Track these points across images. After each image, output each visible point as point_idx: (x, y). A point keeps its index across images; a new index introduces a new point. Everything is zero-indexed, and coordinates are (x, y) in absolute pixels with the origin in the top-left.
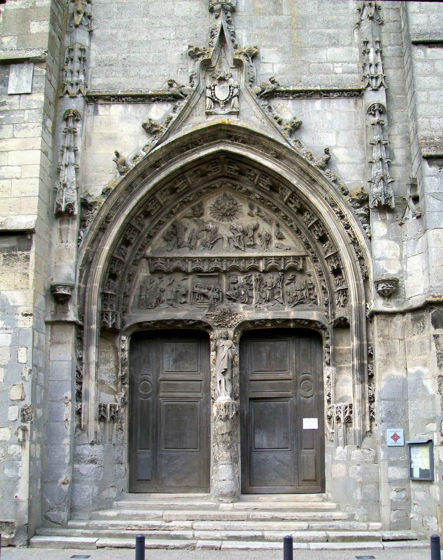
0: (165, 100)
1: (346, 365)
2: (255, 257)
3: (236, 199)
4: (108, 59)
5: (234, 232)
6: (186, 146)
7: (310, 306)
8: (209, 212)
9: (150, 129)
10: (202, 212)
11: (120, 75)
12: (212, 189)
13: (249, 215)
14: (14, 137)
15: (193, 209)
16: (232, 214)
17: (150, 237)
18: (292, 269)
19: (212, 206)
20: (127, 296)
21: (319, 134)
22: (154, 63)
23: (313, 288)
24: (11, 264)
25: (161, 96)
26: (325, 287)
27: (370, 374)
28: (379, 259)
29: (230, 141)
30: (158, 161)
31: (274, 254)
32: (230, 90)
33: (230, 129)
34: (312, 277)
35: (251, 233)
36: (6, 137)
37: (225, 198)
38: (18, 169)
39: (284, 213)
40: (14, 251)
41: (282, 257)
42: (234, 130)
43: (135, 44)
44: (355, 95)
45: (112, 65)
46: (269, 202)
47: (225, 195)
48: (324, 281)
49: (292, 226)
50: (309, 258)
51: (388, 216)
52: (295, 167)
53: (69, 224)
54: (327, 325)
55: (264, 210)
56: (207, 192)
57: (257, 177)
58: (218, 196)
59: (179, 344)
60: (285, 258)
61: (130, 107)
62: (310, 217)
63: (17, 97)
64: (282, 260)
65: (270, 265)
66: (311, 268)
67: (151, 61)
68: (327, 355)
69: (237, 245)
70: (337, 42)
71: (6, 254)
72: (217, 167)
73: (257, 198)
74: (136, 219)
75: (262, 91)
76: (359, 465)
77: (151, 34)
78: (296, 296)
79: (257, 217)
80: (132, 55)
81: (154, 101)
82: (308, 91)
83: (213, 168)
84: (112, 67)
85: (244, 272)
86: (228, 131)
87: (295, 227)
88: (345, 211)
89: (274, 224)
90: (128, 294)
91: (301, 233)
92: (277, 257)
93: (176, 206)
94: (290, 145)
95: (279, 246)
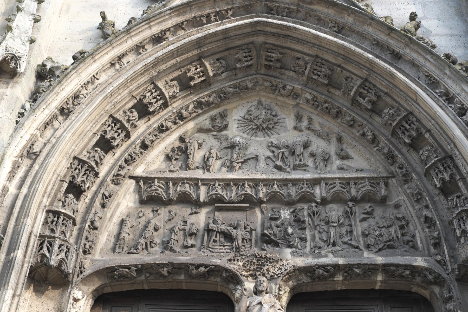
3: (277, 108)
7: (406, 251)
8: (236, 126)
10: (225, 123)
12: (241, 91)
13: (295, 128)
15: (213, 119)
16: (270, 126)
17: (144, 146)
20: (96, 228)
21: (397, 6)
23: (407, 224)
26: (429, 215)
30: (165, 31)
31: (337, 175)
34: (403, 208)
35: (299, 150)
37: (260, 107)
39: (350, 116)
41: (350, 179)
46: (325, 102)
47: (260, 103)
48: (427, 207)
49: (364, 135)
50: (394, 180)
52: (367, 43)
54: (444, 275)
55: (319, 121)
56: (234, 94)
57: (309, 66)
62: (395, 112)
64: (352, 184)
65: (332, 191)
66: (399, 195)
69: (279, 163)
73: (307, 101)
74: (125, 112)
78: (381, 235)
79: (308, 132)
85: (289, 204)
87: (369, 133)
89: (334, 139)
90: (97, 224)
91: (379, 143)
92: (344, 179)
93: (188, 106)
95: (345, 167)
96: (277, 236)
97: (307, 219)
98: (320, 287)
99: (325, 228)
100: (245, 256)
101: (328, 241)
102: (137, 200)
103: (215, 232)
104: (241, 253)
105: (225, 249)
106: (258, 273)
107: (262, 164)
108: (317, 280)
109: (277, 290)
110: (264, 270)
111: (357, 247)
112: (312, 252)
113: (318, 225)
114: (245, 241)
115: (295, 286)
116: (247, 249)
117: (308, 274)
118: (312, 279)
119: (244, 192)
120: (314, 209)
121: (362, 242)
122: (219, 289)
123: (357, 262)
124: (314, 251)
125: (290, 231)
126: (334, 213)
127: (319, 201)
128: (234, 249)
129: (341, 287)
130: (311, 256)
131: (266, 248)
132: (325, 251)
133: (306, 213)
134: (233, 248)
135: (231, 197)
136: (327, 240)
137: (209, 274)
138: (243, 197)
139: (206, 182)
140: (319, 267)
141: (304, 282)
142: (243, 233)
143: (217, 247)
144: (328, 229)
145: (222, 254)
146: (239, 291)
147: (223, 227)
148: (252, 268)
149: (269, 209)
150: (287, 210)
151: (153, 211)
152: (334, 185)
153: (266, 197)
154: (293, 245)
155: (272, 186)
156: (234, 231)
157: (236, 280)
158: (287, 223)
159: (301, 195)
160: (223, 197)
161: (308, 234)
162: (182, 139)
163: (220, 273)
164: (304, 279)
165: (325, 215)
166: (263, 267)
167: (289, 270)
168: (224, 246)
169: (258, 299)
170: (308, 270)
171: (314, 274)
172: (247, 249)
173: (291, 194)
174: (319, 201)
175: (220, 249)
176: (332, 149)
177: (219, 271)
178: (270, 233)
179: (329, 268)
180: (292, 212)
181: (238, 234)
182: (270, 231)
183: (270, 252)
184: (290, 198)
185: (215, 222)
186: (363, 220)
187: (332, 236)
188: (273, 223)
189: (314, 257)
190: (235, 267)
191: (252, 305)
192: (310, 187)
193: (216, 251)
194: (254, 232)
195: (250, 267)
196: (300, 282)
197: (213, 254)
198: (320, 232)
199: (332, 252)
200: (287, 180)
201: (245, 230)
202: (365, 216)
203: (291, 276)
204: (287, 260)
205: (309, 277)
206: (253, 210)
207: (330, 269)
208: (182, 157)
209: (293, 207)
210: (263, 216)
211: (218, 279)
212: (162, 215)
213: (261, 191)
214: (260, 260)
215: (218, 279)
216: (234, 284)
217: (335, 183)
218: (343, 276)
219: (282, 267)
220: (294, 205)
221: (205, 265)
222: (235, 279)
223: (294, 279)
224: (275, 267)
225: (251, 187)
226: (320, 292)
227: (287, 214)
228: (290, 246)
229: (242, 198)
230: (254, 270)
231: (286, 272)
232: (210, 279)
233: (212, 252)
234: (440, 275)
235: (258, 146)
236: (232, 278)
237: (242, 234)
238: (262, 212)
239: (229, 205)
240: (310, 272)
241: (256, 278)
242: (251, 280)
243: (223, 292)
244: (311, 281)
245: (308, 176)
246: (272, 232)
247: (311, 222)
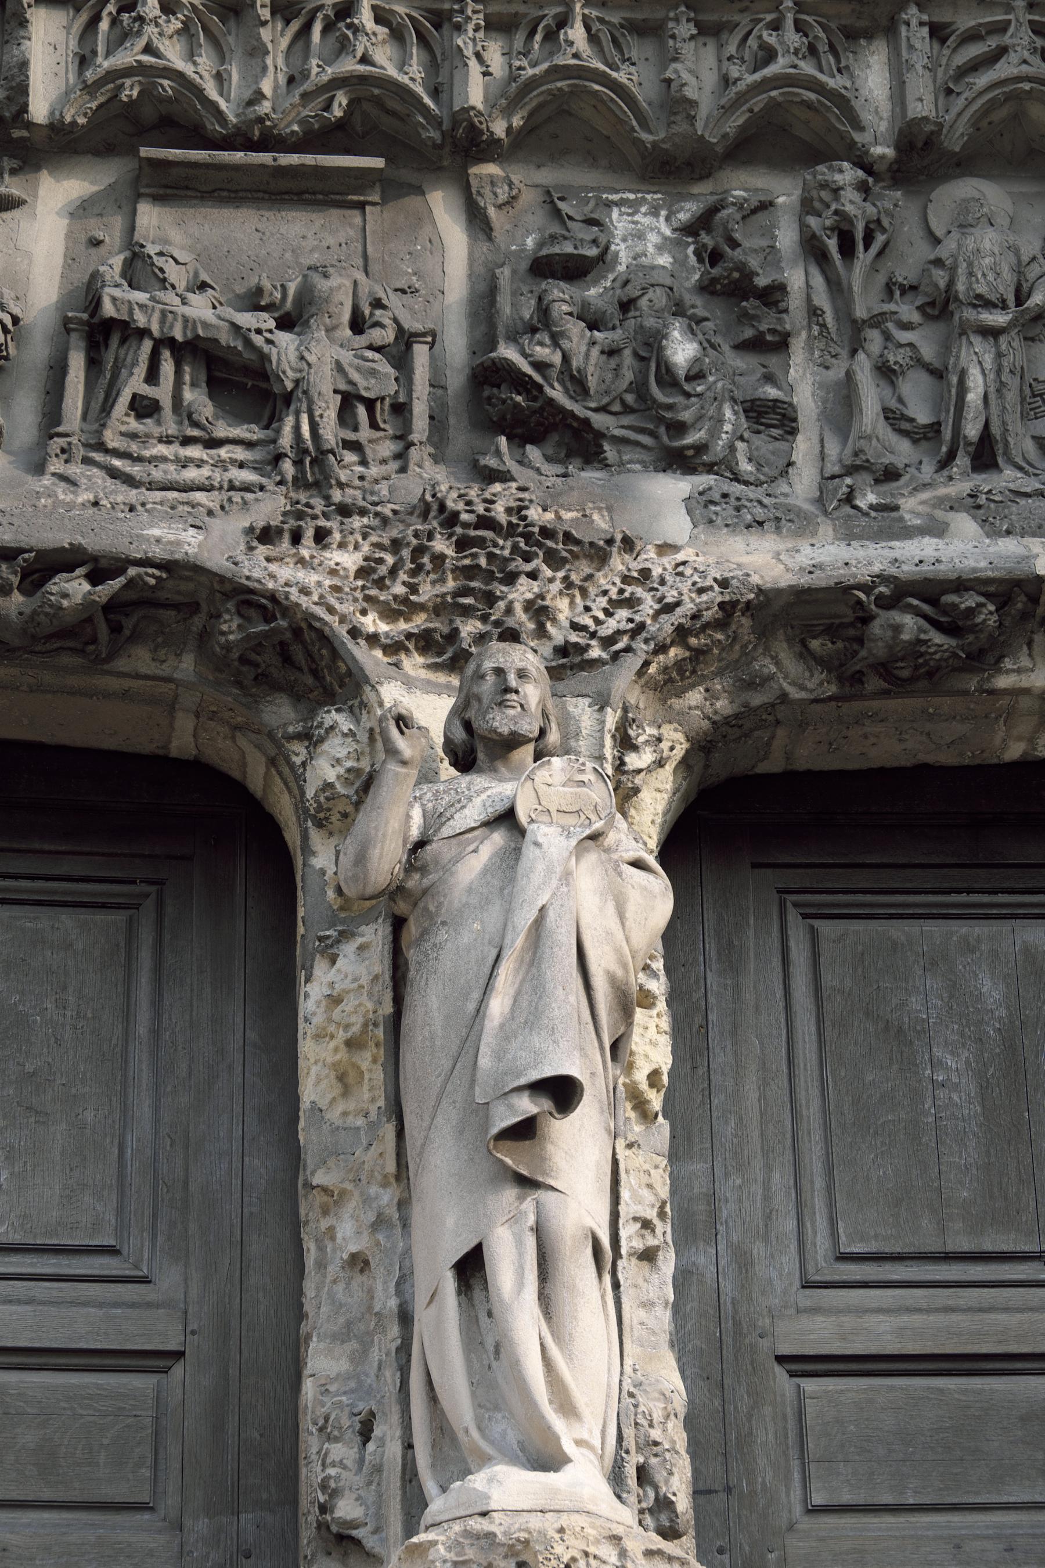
65: (983, 80)
85: (670, 168)
96: (592, 382)
97: (797, 278)
98: (893, 736)
99: (925, 341)
100: (363, 512)
101: (947, 433)
103: (147, 345)
104: (337, 496)
105: (221, 464)
106: (469, 628)
108: (874, 683)
109: (608, 742)
110: (509, 610)
112: (836, 500)
113: (877, 321)
114: (361, 411)
115: (727, 721)
116: (374, 471)
117: (815, 644)
118: (840, 679)
119: (349, 66)
120: (851, 203)
122: (183, 739)
124: (849, 499)
125: (682, 351)
126: (988, 240)
127: (883, 150)
128: (288, 467)
129: (1032, 740)
130: (826, 529)
131: (511, 465)
132: (925, 495)
133: (787, 238)
134: (278, 458)
135: (259, 96)
136: (935, 428)
137: (116, 629)
138: (342, 99)
140: (900, 592)
141: (784, 697)
142: (346, 357)
143: (162, 449)
144: (946, 348)
145: (199, 496)
146: (336, 747)
147: (200, 308)
148: (427, 592)
149: (528, 197)
150: (654, 212)
152: (993, 42)
153: (508, 112)
154: (701, 448)
155: (551, 36)
156: (284, 338)
157: (315, 673)
158: (659, 297)
159: (758, 102)
160: (199, 92)
161: (803, 382)
163: (198, 622)
164: (791, 674)
165: (923, 251)
166: (499, 589)
167: (688, 607)
168: (213, 443)
169: (486, 792)
171: (860, 641)
172: (374, 471)
173: (690, 93)
174: (883, 150)
175: (184, 463)
177: (194, 607)
178: (540, 366)
179: (970, 600)
180: (690, 230)
181: (318, 360)
182: (542, 352)
183: (536, 488)
184: (681, 127)
185: (139, 268)
187: (973, 397)
188: (562, 296)
189: (849, 537)
190: (311, 578)
191: (446, 831)
192: (822, 48)
193: (157, 474)
194: (421, 353)
195: (413, 589)
196: (757, 699)
197: (133, 495)
198: (886, 372)
199: (973, 503)
201: (362, 340)
203: (698, 654)
204: (665, 548)
205: (822, 662)
206: (412, 202)
207: (971, 612)
209: (696, 189)
210: (485, 247)
211: (186, 666)
213: (473, 63)
214: (481, 542)
215: (186, 666)
216: (297, 697)
217: (1001, 28)
219: (639, 591)
220: (702, 178)
221: (95, 559)
222: (304, 664)
223: (719, 673)
224: (584, 592)
225: (397, 35)
226: (882, 772)
227: (653, 238)
228: (679, 461)
229: (338, 112)
230: (439, 609)
231: (667, 624)
232: (121, 664)
233: (130, 481)
236: (287, 659)
237: (339, 367)
238: (477, 220)
239: (238, 157)
240: (832, 631)
241: (457, 662)
242: (424, 674)
243: (211, 756)
244: (832, 689)
246: (557, 359)
247: (822, 299)
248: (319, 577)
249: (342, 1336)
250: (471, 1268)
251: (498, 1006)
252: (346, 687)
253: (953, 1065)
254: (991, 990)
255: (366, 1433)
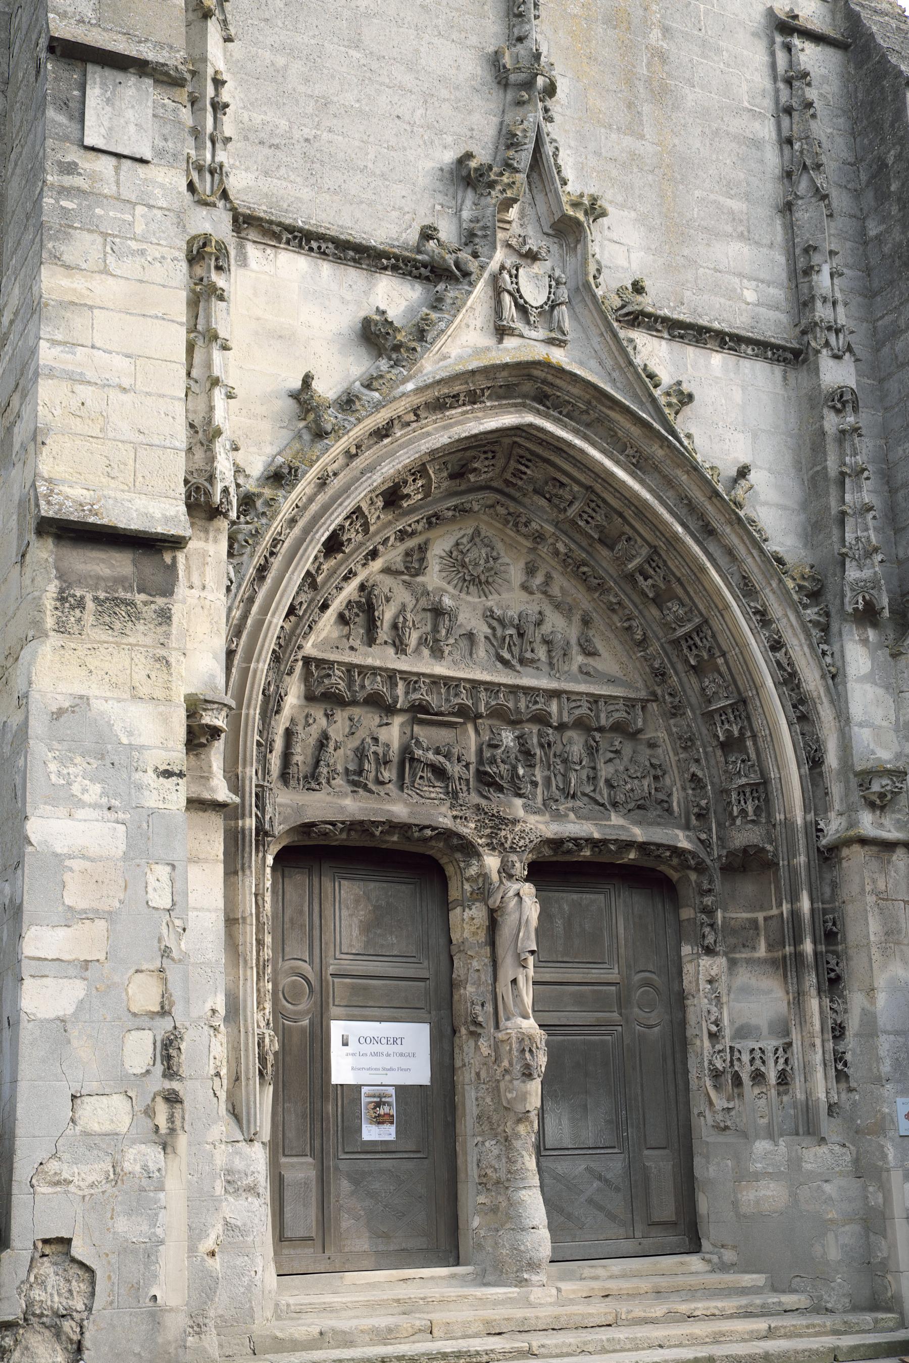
0: (410, 274)
1: (744, 956)
2: (545, 691)
3: (499, 546)
4: (268, 128)
5: (495, 624)
6: (454, 397)
7: (659, 816)
8: (437, 568)
9: (375, 336)
11: (298, 179)
13: (525, 587)
14: (105, 271)
18: (618, 728)
19: (444, 554)
22: (378, 172)
24: (118, 625)
25: (406, 260)
26: (700, 774)
27: (832, 975)
28: (861, 725)
29: (541, 408)
31: (582, 688)
32: (550, 286)
33: (550, 378)
34: (660, 751)
36: (84, 266)
38: (120, 363)
39: (616, 595)
40: (125, 590)
41: (601, 696)
42: (558, 382)
43: (332, 109)
44: (785, 360)
45: (277, 147)
48: (697, 761)
50: (654, 705)
51: (871, 634)
52: (670, 493)
53: (207, 540)
55: (561, 583)
58: (462, 532)
59: (372, 885)
60: (608, 699)
61: (326, 268)
63: (112, 161)
64: (601, 703)
66: (658, 730)
67: (370, 165)
68: (707, 930)
70: (746, 233)
71: (102, 595)
72: (492, 462)
73: (556, 553)
75: (623, 307)
76: (826, 1181)
77: (369, 96)
79: (541, 596)
80: (325, 136)
81: (385, 268)
82: (705, 328)
83: (487, 463)
84: (278, 152)
85: (514, 723)
86: (544, 382)
88: (776, 609)
89: (577, 618)
92: (592, 695)
94: (681, 443)
97: (538, 751)
102: (302, 694)
107: (481, 652)
111: (603, 805)
121: (606, 796)
123: (614, 837)
133: (535, 740)
134: (448, 793)
139: (405, 675)
144: (566, 770)
146: (474, 868)
151: (327, 715)
152: (579, 703)
162: (362, 587)
165: (561, 746)
170: (556, 844)
176: (573, 633)
180: (518, 737)
186: (610, 760)
197: (423, 800)
200: (518, 687)
202: (612, 755)
208: (361, 620)
212: (339, 724)
218: (592, 850)
222: (469, 850)
228: (520, 796)
231: (531, 846)
234: (704, 861)
235: (469, 612)
238: (477, 731)
245: (544, 683)
248: (468, 830)
249: (474, 984)
250: (514, 981)
251: (521, 934)
252: (479, 855)
253: (559, 922)
254: (566, 907)
255: (483, 1005)
